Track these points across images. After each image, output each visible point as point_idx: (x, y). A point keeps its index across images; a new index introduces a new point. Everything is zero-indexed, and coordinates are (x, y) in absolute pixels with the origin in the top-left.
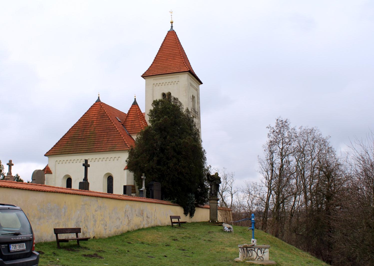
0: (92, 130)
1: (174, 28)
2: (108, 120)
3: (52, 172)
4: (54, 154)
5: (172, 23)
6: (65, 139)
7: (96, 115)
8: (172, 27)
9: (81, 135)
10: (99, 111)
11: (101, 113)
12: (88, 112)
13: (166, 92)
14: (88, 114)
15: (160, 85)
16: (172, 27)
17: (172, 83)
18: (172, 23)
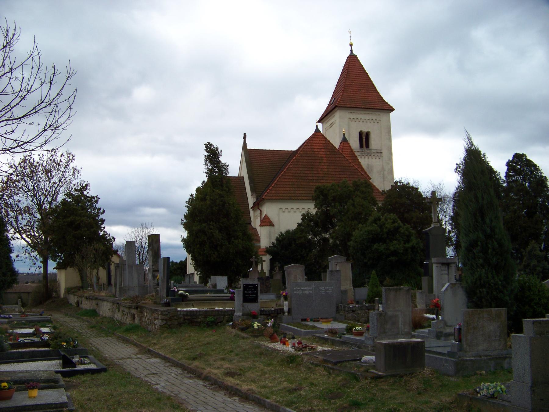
0: (326, 170)
1: (355, 53)
2: (343, 159)
3: (274, 223)
4: (277, 198)
5: (351, 45)
6: (287, 177)
7: (323, 150)
8: (351, 50)
9: (310, 175)
10: (325, 145)
11: (328, 147)
12: (309, 144)
13: (365, 130)
14: (309, 147)
15: (357, 121)
16: (351, 50)
17: (372, 121)
18: (351, 45)
